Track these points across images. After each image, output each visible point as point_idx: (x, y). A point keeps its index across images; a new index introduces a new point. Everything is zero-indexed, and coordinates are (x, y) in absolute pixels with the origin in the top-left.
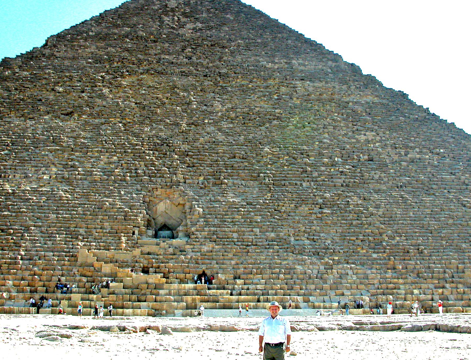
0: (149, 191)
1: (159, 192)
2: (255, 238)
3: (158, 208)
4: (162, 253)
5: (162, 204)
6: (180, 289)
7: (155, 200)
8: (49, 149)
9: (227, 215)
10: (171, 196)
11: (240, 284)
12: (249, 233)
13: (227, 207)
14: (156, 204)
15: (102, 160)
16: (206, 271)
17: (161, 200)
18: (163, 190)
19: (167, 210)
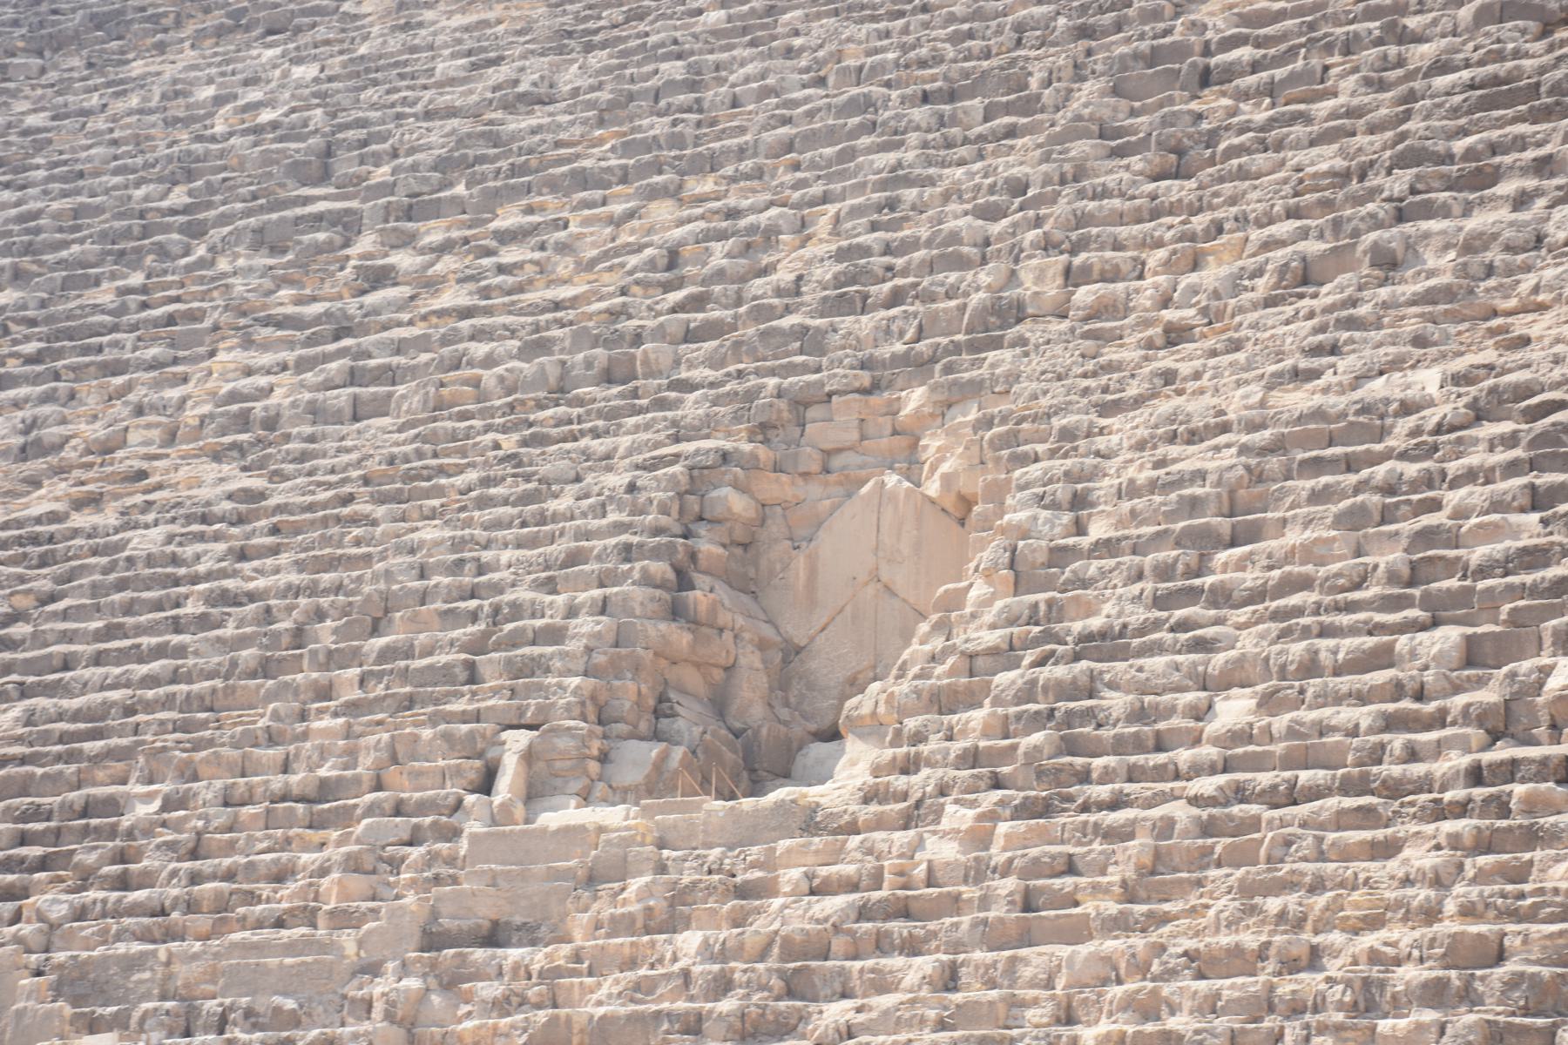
7: (814, 490)
8: (259, 231)
15: (563, 248)
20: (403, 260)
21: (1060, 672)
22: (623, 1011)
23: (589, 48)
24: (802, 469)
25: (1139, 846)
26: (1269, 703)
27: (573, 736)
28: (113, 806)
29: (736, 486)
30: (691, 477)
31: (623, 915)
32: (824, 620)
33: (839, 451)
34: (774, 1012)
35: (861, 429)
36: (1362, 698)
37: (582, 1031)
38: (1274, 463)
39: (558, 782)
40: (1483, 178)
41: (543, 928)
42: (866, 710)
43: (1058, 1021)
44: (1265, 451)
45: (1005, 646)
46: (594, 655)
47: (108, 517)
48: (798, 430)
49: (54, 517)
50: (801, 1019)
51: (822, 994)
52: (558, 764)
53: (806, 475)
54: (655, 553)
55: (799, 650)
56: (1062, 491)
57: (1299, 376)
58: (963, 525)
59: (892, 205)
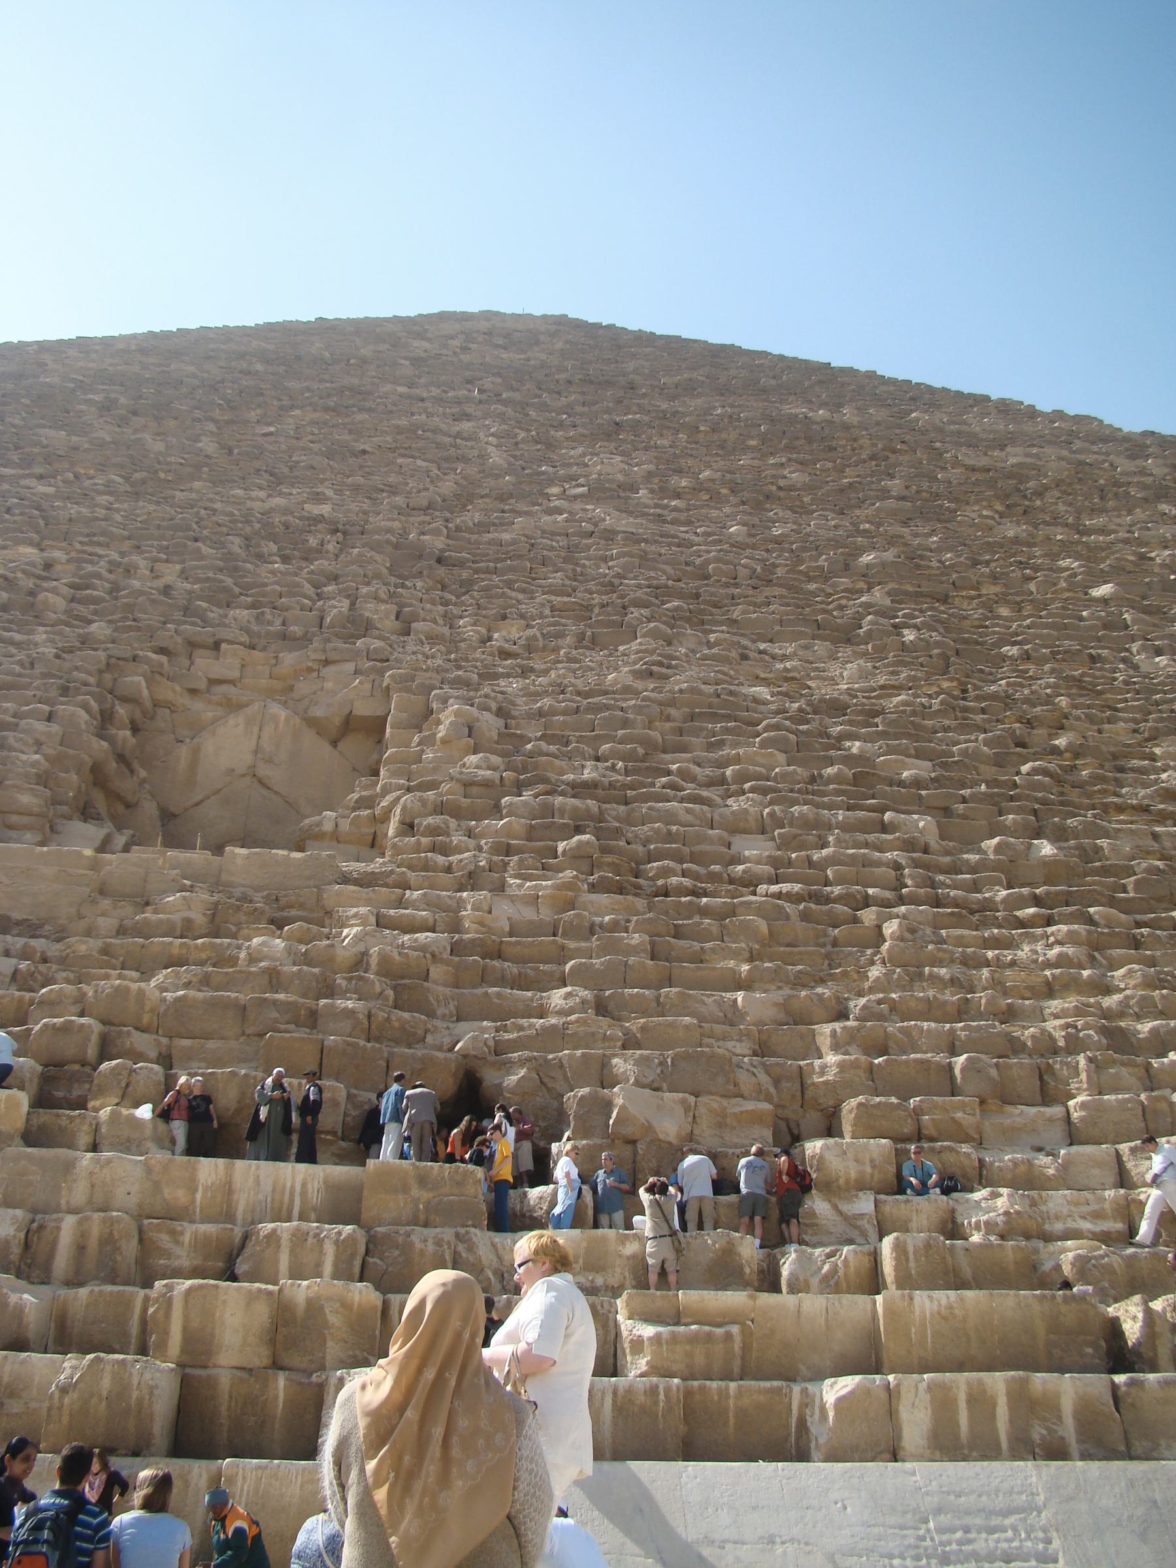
0: (162, 651)
1: (227, 665)
2: (916, 864)
3: (209, 745)
4: (106, 924)
5: (235, 726)
6: (174, 1215)
7: (197, 705)
9: (684, 749)
10: (304, 687)
11: (862, 1186)
12: (861, 837)
13: (672, 711)
14: (198, 728)
16: (489, 1077)
17: (232, 707)
18: (256, 654)
19: (269, 761)
22: (201, 995)
24: (192, 686)
26: (785, 844)
27: (36, 796)
30: (108, 664)
31: (161, 921)
32: (200, 797)
33: (220, 682)
34: (399, 1020)
35: (241, 672)
37: (152, 1010)
39: (13, 834)
41: (47, 927)
42: (328, 827)
43: (755, 1054)
45: (498, 782)
46: (44, 747)
48: (187, 662)
50: (426, 1031)
51: (439, 1012)
52: (14, 819)
53: (193, 692)
55: (174, 816)
58: (335, 747)
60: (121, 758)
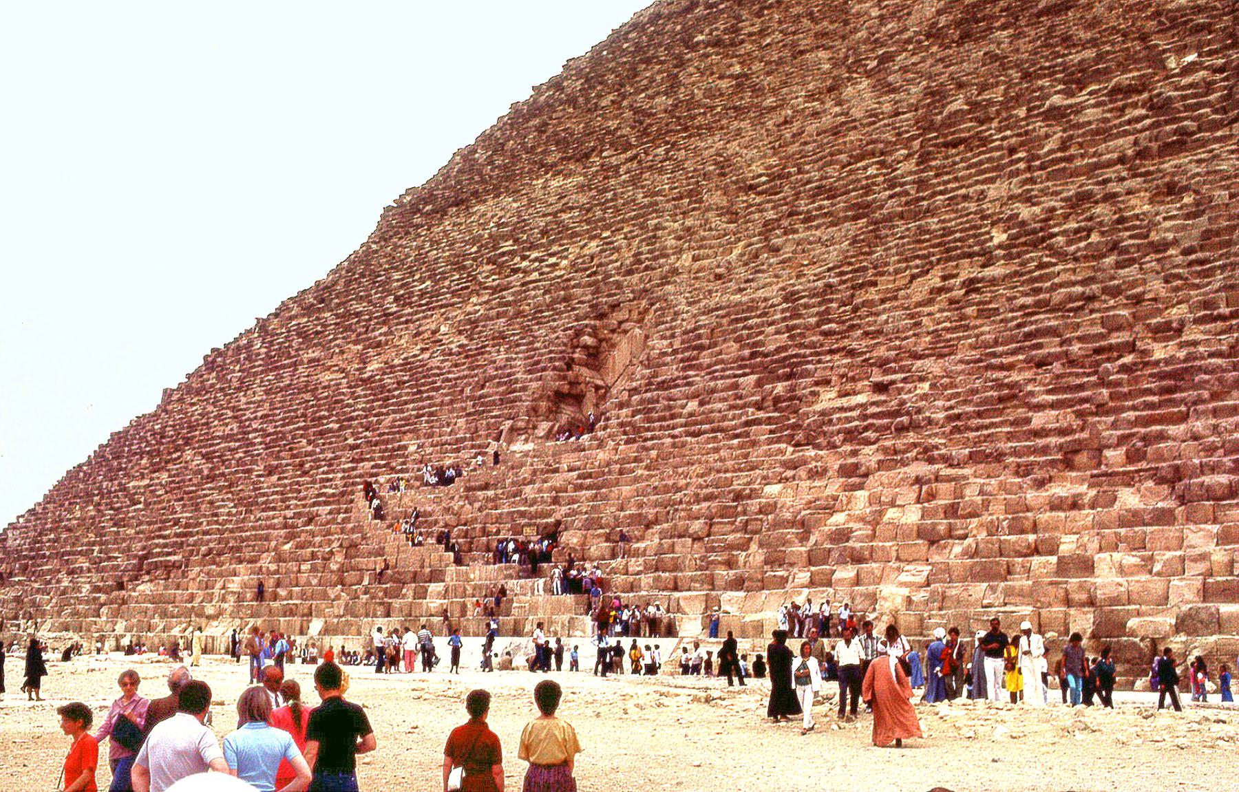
15: (566, 258)
20: (525, 264)
21: (649, 395)
23: (591, 190)
25: (654, 453)
26: (702, 404)
28: (405, 447)
29: (589, 335)
36: (725, 400)
38: (725, 321)
40: (808, 219)
44: (723, 317)
47: (426, 355)
49: (415, 356)
54: (560, 359)
56: (668, 333)
57: (741, 290)
59: (654, 237)
60: (570, 383)
